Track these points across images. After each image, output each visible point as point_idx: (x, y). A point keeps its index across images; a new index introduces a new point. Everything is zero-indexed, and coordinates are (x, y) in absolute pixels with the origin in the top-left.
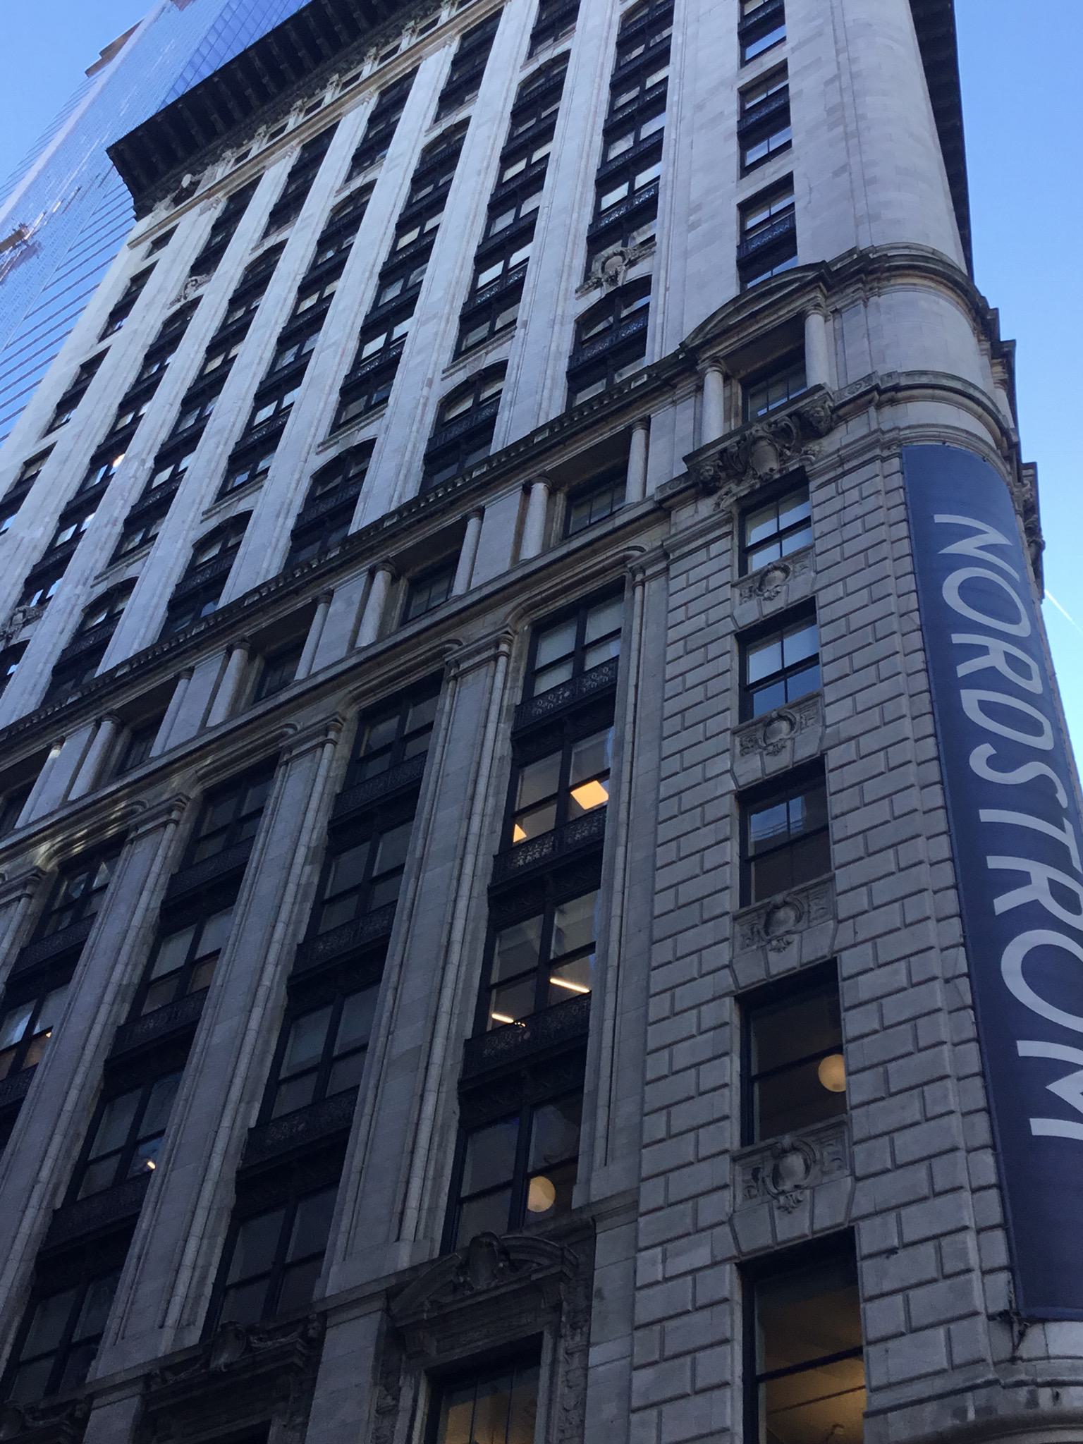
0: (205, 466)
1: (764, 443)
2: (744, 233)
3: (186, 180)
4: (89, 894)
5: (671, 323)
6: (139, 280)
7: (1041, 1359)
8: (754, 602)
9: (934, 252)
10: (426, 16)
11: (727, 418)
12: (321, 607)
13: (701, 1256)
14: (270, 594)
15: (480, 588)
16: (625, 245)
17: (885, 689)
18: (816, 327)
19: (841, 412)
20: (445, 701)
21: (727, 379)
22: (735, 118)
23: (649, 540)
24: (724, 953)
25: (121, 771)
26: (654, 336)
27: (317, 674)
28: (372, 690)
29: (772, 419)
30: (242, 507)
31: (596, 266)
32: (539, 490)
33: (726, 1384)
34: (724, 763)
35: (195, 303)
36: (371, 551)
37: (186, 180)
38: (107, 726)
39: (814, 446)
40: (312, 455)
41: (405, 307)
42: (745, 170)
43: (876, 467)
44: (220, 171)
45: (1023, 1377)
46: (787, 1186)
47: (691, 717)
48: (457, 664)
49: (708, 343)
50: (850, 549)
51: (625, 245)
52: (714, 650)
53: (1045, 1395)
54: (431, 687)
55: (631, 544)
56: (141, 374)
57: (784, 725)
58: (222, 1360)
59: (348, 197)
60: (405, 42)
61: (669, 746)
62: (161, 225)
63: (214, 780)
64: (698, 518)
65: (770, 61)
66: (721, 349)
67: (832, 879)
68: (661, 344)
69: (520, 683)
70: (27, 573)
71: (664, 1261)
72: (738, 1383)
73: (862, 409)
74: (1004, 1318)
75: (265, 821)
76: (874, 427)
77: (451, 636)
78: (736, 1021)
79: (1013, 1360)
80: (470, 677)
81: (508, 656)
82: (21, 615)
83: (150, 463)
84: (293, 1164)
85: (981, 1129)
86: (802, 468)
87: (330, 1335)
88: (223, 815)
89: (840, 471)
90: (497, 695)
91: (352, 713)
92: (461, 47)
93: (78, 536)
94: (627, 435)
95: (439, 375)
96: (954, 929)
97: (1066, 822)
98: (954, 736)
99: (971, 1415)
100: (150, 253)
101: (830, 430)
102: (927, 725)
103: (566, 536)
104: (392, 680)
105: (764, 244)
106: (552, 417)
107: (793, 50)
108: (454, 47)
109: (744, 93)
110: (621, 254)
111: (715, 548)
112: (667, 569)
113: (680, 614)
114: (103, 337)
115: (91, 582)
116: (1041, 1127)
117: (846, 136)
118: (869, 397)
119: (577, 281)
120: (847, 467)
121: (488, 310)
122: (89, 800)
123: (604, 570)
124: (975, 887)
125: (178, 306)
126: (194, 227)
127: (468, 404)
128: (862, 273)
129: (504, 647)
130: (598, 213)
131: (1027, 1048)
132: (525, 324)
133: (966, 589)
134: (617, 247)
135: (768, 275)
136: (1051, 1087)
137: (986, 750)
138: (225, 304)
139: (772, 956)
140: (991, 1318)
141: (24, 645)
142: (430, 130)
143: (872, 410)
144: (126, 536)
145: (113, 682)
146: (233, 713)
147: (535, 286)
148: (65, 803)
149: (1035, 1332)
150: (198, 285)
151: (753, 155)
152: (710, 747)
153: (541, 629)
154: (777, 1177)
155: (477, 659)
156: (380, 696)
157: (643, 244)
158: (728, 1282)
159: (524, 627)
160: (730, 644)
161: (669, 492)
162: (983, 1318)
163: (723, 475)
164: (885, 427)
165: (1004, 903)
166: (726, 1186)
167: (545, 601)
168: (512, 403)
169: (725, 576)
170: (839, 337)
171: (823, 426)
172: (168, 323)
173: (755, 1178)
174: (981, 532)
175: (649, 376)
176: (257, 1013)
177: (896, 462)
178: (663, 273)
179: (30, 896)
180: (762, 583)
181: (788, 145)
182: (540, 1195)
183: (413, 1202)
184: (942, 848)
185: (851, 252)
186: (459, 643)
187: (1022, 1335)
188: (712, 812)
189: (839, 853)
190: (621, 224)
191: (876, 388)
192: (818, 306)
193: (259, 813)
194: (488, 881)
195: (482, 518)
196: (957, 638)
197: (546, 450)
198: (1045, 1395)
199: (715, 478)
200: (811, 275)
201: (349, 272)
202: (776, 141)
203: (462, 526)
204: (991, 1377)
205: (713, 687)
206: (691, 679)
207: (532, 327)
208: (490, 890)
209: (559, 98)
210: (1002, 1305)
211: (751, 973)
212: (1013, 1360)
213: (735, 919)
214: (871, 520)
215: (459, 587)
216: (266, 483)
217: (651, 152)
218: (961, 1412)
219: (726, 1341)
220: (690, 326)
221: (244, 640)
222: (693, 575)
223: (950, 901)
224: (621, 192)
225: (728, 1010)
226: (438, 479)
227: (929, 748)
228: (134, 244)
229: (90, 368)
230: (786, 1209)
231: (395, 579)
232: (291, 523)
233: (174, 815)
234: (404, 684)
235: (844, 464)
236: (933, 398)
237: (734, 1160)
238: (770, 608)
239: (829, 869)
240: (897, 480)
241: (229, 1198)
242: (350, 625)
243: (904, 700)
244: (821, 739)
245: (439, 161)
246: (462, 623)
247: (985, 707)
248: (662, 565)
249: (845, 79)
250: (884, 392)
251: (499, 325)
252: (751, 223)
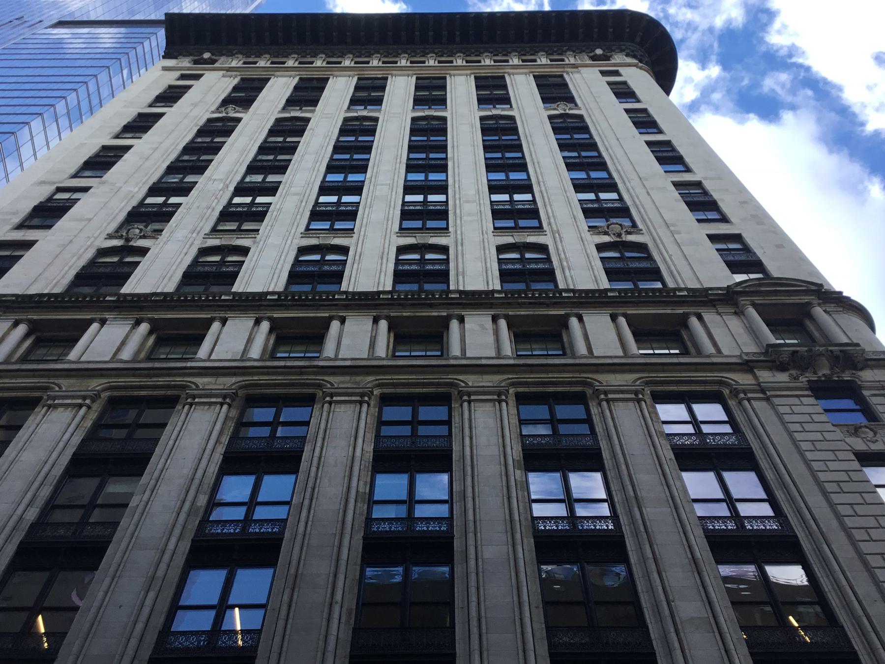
3: (207, 55)
19: (869, 363)
28: (527, 384)
29: (830, 348)
40: (394, 237)
66: (758, 300)
70: (129, 208)
83: (231, 188)
171: (860, 366)
199: (788, 364)
200: (814, 288)
234: (552, 389)
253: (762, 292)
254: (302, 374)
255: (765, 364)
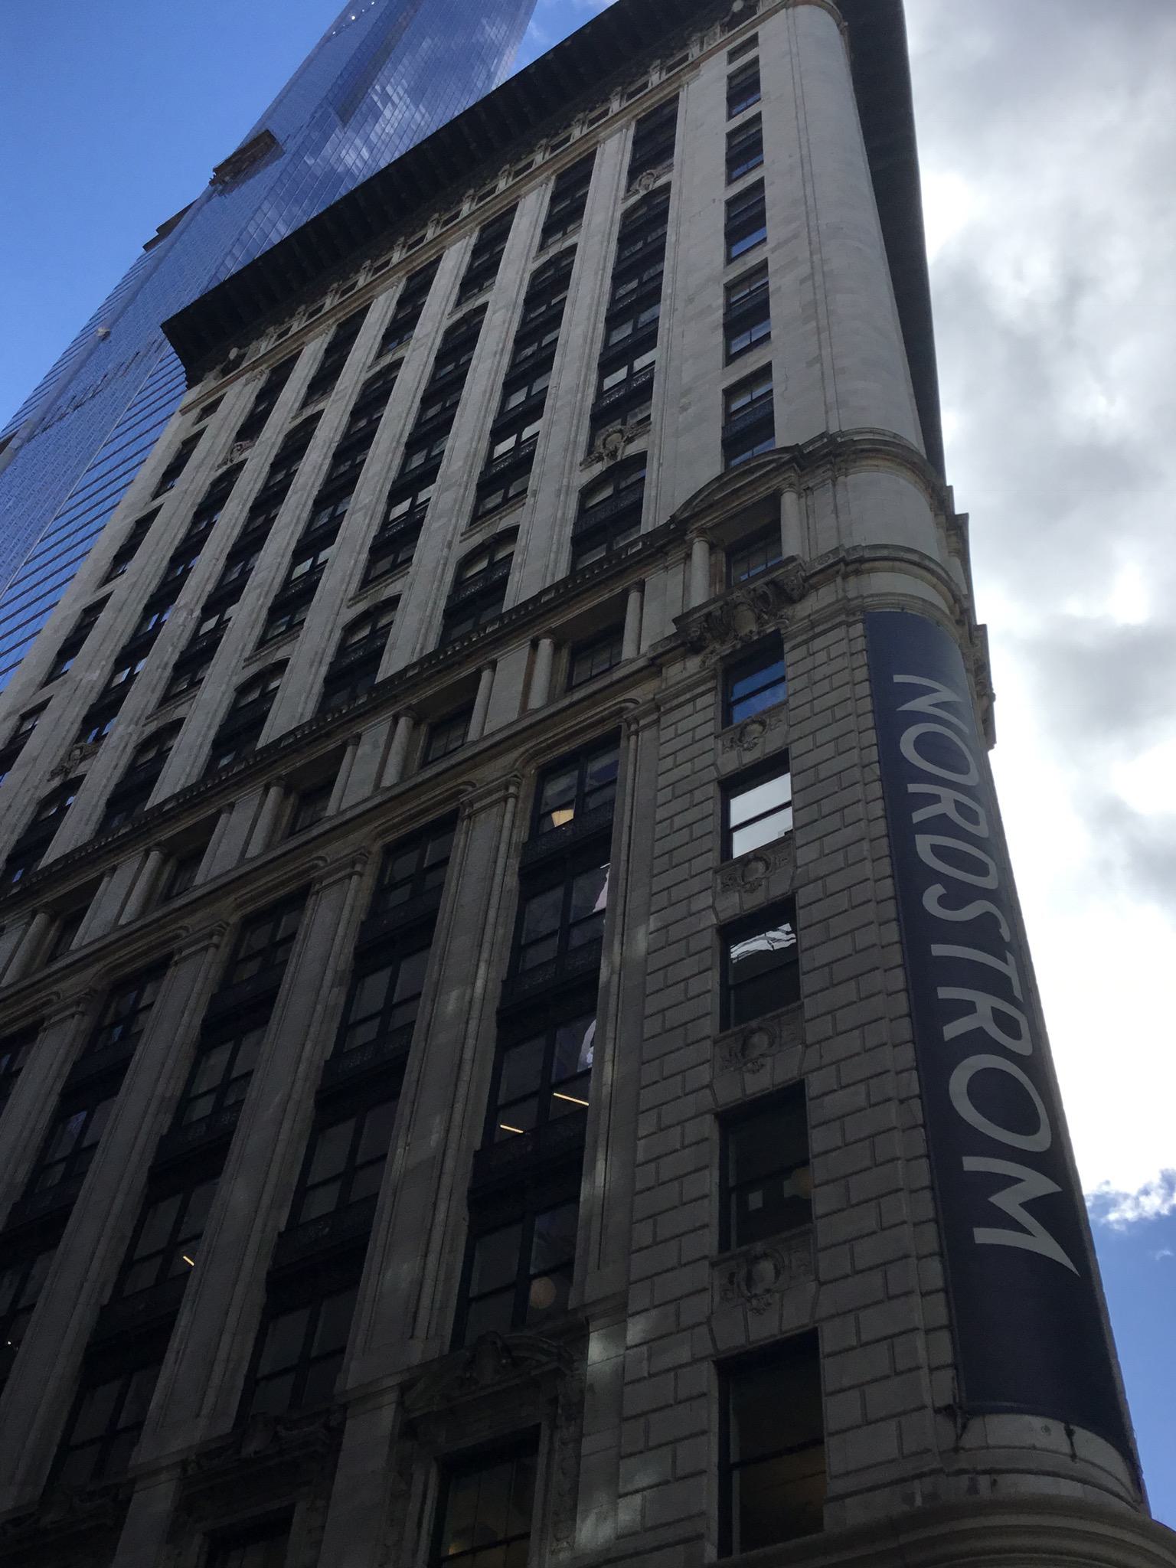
0: (246, 615)
1: (741, 608)
2: (728, 415)
3: (233, 354)
4: (136, 1011)
5: (664, 496)
6: (189, 445)
7: (982, 1448)
8: (734, 753)
9: (895, 436)
10: (447, 210)
11: (712, 584)
12: (350, 749)
13: (684, 1355)
14: (304, 736)
15: (492, 734)
16: (624, 423)
17: (849, 834)
18: (789, 500)
19: (812, 581)
20: (459, 839)
21: (712, 548)
22: (721, 312)
23: (643, 693)
24: (705, 1074)
25: (167, 897)
26: (648, 509)
27: (345, 811)
28: (395, 827)
30: (280, 655)
31: (599, 442)
32: (545, 644)
33: (702, 1472)
34: (706, 899)
35: (240, 466)
36: (395, 699)
37: (233, 354)
38: (155, 856)
39: (788, 611)
40: (344, 610)
41: (428, 474)
42: (730, 359)
43: (840, 632)
44: (264, 346)
45: (964, 1466)
46: (758, 1290)
47: (678, 856)
48: (471, 804)
49: (695, 516)
50: (818, 705)
51: (624, 423)
52: (698, 796)
53: (984, 1481)
54: (446, 825)
55: (628, 696)
56: (190, 530)
57: (761, 866)
58: (250, 1448)
59: (380, 372)
60: (430, 233)
61: (658, 884)
62: (209, 394)
63: (250, 908)
64: (686, 674)
65: (753, 260)
66: (707, 521)
67: (801, 1006)
68: (652, 519)
69: (527, 823)
70: (84, 713)
71: (649, 1358)
72: (715, 1470)
73: (831, 580)
74: (948, 1411)
75: (297, 947)
76: (841, 594)
77: (464, 778)
78: (715, 1136)
79: (956, 1449)
80: (483, 815)
81: (517, 797)
82: (77, 752)
83: (197, 613)
84: (318, 1265)
85: (930, 1237)
86: (777, 632)
87: (349, 1423)
88: (259, 939)
89: (811, 634)
90: (506, 834)
91: (377, 847)
92: (480, 238)
93: (131, 678)
94: (624, 596)
95: (458, 538)
96: (908, 1055)
97: (1009, 956)
98: (909, 876)
99: (919, 1501)
100: (200, 419)
101: (802, 597)
102: (885, 867)
103: (570, 688)
104: (412, 818)
105: (747, 425)
106: (558, 578)
107: (773, 250)
108: (473, 240)
109: (730, 288)
110: (620, 431)
111: (701, 703)
112: (657, 721)
113: (669, 762)
114: (156, 495)
115: (143, 721)
116: (984, 1236)
117: (819, 331)
118: (836, 568)
119: (580, 456)
120: (817, 630)
121: (503, 479)
122: (138, 924)
123: (603, 720)
124: (928, 1015)
125: (225, 468)
126: (239, 397)
127: (484, 564)
128: (831, 455)
129: (512, 790)
130: (600, 393)
131: (972, 1163)
132: (535, 493)
133: (920, 743)
134: (617, 425)
135: (748, 454)
136: (992, 1199)
137: (936, 890)
138: (267, 468)
139: (748, 1076)
140: (937, 1411)
141: (81, 778)
142: (451, 314)
143: (839, 580)
144: (174, 680)
145: (163, 815)
146: (268, 846)
147: (544, 460)
148: (116, 926)
149: (976, 1424)
150: (242, 450)
151: (738, 345)
152: (695, 884)
153: (547, 773)
154: (750, 1280)
155: (488, 800)
156: (403, 831)
157: (640, 422)
158: (706, 1378)
159: (531, 770)
160: (712, 790)
161: (660, 650)
162: (930, 1411)
163: (708, 635)
164: (851, 595)
165: (952, 1030)
166: (705, 1289)
167: (550, 747)
168: (523, 565)
169: (709, 728)
170: (808, 514)
171: (796, 594)
172: (215, 484)
173: (731, 1282)
174: (934, 691)
175: (644, 544)
176: (286, 1125)
177: (860, 626)
178: (656, 451)
179: (83, 1014)
180: (742, 734)
181: (768, 336)
182: (541, 1292)
183: (425, 1301)
184: (898, 979)
185: (822, 436)
186: (473, 785)
187: (964, 1427)
188: (695, 944)
189: (808, 984)
190: (621, 405)
191: (843, 560)
192: (791, 485)
193: (291, 937)
194: (497, 1003)
195: (494, 670)
196: (912, 788)
197: (551, 609)
198: (984, 1481)
199: (701, 638)
200: (786, 457)
201: (378, 443)
202: (758, 333)
203: (476, 677)
204: (935, 1465)
205: (698, 830)
206: (678, 822)
207: (540, 496)
208: (498, 1012)
209: (567, 287)
210: (946, 1399)
211: (729, 1093)
212: (956, 1449)
213: (715, 1042)
214: (837, 680)
215: (473, 734)
216: (302, 633)
217: (647, 340)
218: (909, 1499)
219: (704, 1433)
220: (680, 501)
221: (280, 778)
222: (682, 726)
223: (905, 1028)
224: (622, 374)
225: (709, 1127)
226: (456, 633)
227: (887, 887)
228: (185, 411)
229: (143, 524)
230: (758, 1311)
231: (416, 725)
232: (324, 670)
233: (215, 939)
235: (815, 627)
236: (892, 570)
237: (713, 1265)
238: (749, 758)
239: (799, 999)
240: (861, 644)
241: (259, 1296)
242: (375, 767)
243: (865, 845)
244: (793, 879)
245: (460, 342)
246: (475, 767)
247: (937, 850)
248: (655, 717)
249: (818, 278)
250: (851, 564)
251: (511, 493)
252: (735, 406)
253: (718, 502)
254: (163, 927)
255: (677, 652)
